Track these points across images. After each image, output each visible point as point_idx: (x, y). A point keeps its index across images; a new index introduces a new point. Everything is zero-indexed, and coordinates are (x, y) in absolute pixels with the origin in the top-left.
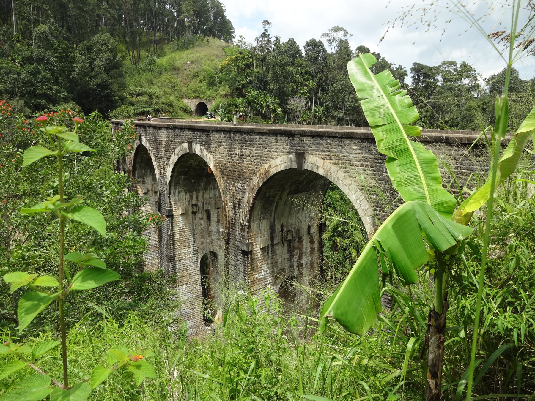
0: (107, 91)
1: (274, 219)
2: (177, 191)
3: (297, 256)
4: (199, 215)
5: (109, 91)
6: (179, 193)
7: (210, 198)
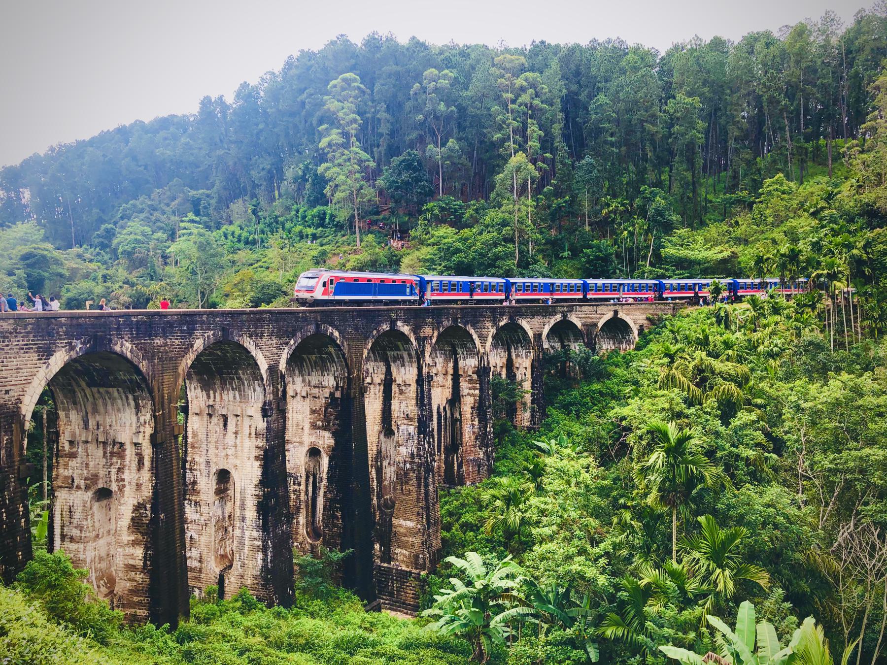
2: (193, 386)
4: (214, 420)
6: (195, 388)
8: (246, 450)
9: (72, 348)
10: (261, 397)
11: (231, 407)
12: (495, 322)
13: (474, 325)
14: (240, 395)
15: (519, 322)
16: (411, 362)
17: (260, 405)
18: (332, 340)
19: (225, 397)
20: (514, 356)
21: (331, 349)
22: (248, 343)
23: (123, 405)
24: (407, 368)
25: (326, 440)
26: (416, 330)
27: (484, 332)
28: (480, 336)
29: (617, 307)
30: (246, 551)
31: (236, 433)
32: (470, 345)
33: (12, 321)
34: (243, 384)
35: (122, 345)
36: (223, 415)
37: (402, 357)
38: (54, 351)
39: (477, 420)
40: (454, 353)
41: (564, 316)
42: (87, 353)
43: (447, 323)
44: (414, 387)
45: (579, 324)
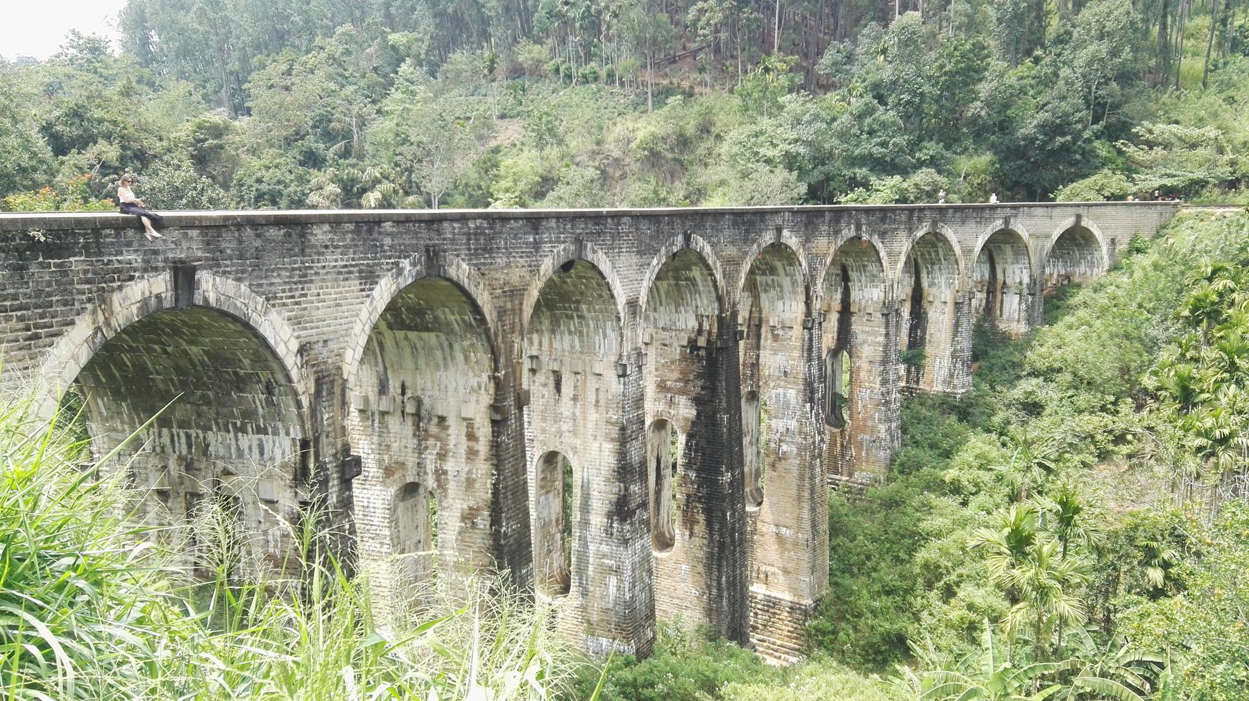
0: (1060, 140)
1: (385, 368)
3: (435, 452)
5: (1069, 138)
7: (563, 350)
8: (591, 425)
9: (400, 272)
10: (615, 345)
11: (567, 360)
12: (910, 231)
13: (882, 235)
14: (581, 341)
15: (944, 231)
16: (794, 292)
17: (614, 358)
18: (702, 259)
19: (556, 344)
20: (925, 283)
21: (696, 273)
22: (604, 265)
23: (445, 359)
24: (788, 303)
25: (685, 410)
26: (806, 241)
27: (896, 247)
28: (889, 254)
29: (1080, 211)
30: (590, 573)
31: (575, 398)
32: (873, 268)
33: (326, 227)
34: (588, 326)
35: (458, 266)
36: (554, 372)
37: (780, 286)
38: (378, 276)
39: (879, 379)
40: (846, 278)
41: (1007, 221)
42: (419, 283)
43: (848, 232)
44: (797, 331)
45: (1024, 235)
